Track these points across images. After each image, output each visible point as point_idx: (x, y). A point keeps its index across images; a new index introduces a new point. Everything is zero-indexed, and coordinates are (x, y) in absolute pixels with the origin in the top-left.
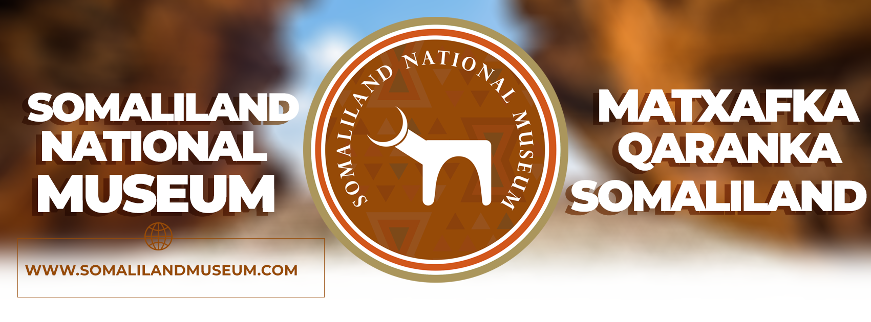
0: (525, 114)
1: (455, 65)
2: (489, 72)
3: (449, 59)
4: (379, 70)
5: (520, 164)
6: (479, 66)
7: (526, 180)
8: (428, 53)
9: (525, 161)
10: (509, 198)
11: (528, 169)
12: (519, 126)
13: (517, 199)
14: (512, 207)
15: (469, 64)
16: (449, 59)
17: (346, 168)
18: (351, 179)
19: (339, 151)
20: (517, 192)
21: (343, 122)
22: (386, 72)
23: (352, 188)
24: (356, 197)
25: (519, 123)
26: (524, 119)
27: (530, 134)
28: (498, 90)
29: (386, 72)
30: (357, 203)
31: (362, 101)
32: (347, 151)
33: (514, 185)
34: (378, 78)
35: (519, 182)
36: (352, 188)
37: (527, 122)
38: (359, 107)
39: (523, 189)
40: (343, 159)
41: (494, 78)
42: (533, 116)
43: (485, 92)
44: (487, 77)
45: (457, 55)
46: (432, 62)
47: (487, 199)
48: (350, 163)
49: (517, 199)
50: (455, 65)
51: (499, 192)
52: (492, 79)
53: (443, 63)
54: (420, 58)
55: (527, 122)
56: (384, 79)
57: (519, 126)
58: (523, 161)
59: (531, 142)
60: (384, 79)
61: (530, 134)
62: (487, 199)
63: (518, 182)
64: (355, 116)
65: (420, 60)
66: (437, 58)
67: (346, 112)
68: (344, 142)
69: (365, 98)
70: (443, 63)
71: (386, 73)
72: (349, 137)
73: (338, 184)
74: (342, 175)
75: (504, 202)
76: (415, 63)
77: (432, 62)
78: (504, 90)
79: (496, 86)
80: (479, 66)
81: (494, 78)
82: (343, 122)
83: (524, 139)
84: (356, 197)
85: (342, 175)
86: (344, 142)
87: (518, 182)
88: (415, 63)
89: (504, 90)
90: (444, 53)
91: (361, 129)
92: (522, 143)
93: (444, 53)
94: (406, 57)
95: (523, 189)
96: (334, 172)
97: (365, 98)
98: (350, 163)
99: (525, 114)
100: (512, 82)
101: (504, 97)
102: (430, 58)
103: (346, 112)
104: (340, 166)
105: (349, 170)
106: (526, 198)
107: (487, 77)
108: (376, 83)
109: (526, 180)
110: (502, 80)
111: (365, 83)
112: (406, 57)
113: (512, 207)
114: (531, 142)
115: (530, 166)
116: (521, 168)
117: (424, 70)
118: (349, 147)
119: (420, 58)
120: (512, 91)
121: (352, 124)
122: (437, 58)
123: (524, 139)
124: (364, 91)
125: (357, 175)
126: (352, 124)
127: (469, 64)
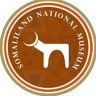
0: (81, 34)
1: (55, 16)
2: (68, 19)
3: (53, 14)
4: (27, 18)
5: (79, 53)
6: (64, 17)
7: (82, 59)
8: (45, 12)
9: (81, 51)
10: (75, 65)
11: (82, 54)
12: (79, 39)
13: (78, 66)
14: (76, 68)
15: (61, 16)
16: (53, 14)
17: (15, 54)
18: (17, 58)
19: (13, 48)
20: (78, 63)
21: (14, 37)
22: (30, 19)
23: (18, 61)
24: (19, 65)
25: (79, 37)
26: (81, 36)
27: (83, 41)
28: (71, 25)
29: (30, 19)
30: (19, 67)
31: (21, 29)
32: (16, 48)
33: (77, 60)
34: (27, 21)
35: (79, 59)
36: (18, 61)
37: (82, 37)
38: (20, 31)
39: (80, 62)
40: (14, 51)
41: (70, 21)
42: (84, 35)
43: (66, 26)
44: (67, 21)
45: (56, 12)
46: (47, 15)
47: (67, 66)
48: (17, 52)
49: (78, 66)
50: (55, 16)
51: (71, 64)
52: (69, 21)
53: (51, 15)
54: (43, 13)
55: (82, 37)
56: (29, 21)
57: (79, 39)
58: (81, 52)
59: (83, 45)
60: (29, 21)
61: (83, 41)
62: (67, 66)
63: (79, 59)
64: (19, 35)
65: (43, 14)
66: (49, 14)
67: (15, 33)
68: (15, 45)
69: (22, 28)
70: (51, 15)
71: (30, 19)
72: (17, 43)
73: (13, 60)
74: (14, 57)
75: (73, 67)
76: (41, 15)
77: (47, 15)
78: (74, 25)
79: (71, 24)
80: (64, 17)
81: (70, 21)
82: (14, 37)
83: (81, 43)
84: (19, 65)
85: (14, 57)
86: (15, 45)
87: (79, 59)
88: (41, 15)
89: (74, 25)
90: (51, 12)
91: (21, 40)
92: (80, 45)
93: (51, 12)
94: (37, 13)
95: (80, 62)
96: (11, 56)
97: (22, 28)
98: (17, 52)
99: (81, 34)
100: (76, 22)
101: (73, 28)
102: (46, 14)
103: (15, 33)
104: (13, 53)
105: (17, 55)
106: (82, 65)
107: (67, 21)
108: (26, 23)
109: (82, 59)
110: (73, 22)
111: (22, 23)
112: (37, 13)
113: (76, 68)
114: (83, 45)
115: (83, 53)
116: (80, 54)
117: (44, 18)
118: (16, 46)
119: (43, 13)
120: (76, 26)
121: (18, 38)
122: (49, 14)
123: (81, 43)
124: (22, 26)
125: (20, 57)
126: (18, 38)
127: (61, 16)
